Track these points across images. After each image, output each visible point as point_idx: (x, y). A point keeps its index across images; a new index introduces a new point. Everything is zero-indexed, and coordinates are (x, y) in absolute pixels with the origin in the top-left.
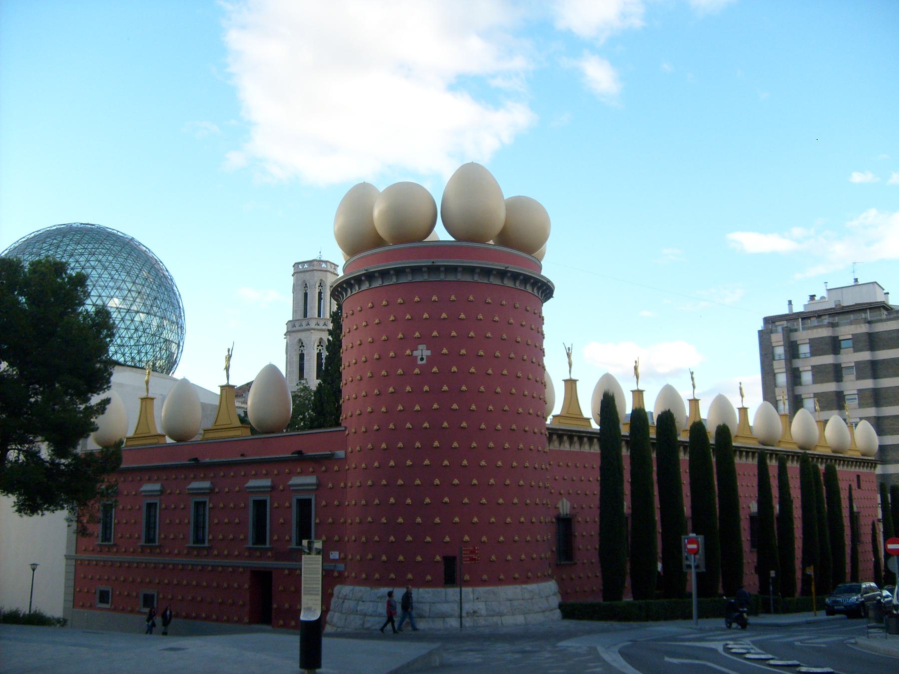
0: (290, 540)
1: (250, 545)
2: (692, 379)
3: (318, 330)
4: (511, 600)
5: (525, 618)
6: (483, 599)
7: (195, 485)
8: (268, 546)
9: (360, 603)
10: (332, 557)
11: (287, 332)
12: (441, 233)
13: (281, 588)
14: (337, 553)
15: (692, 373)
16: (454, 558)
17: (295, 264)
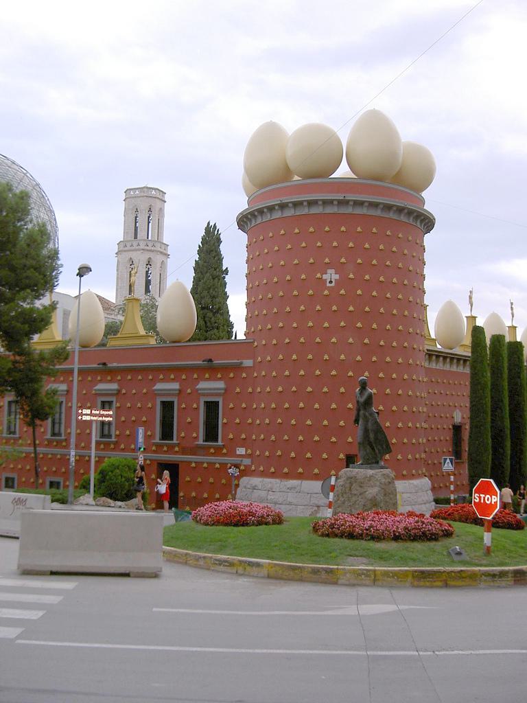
0: (196, 438)
1: (157, 440)
2: (512, 308)
3: (148, 250)
7: (101, 386)
8: (175, 441)
10: (238, 453)
11: (119, 251)
12: (343, 171)
14: (244, 449)
15: (512, 304)
16: (356, 455)
17: (128, 190)
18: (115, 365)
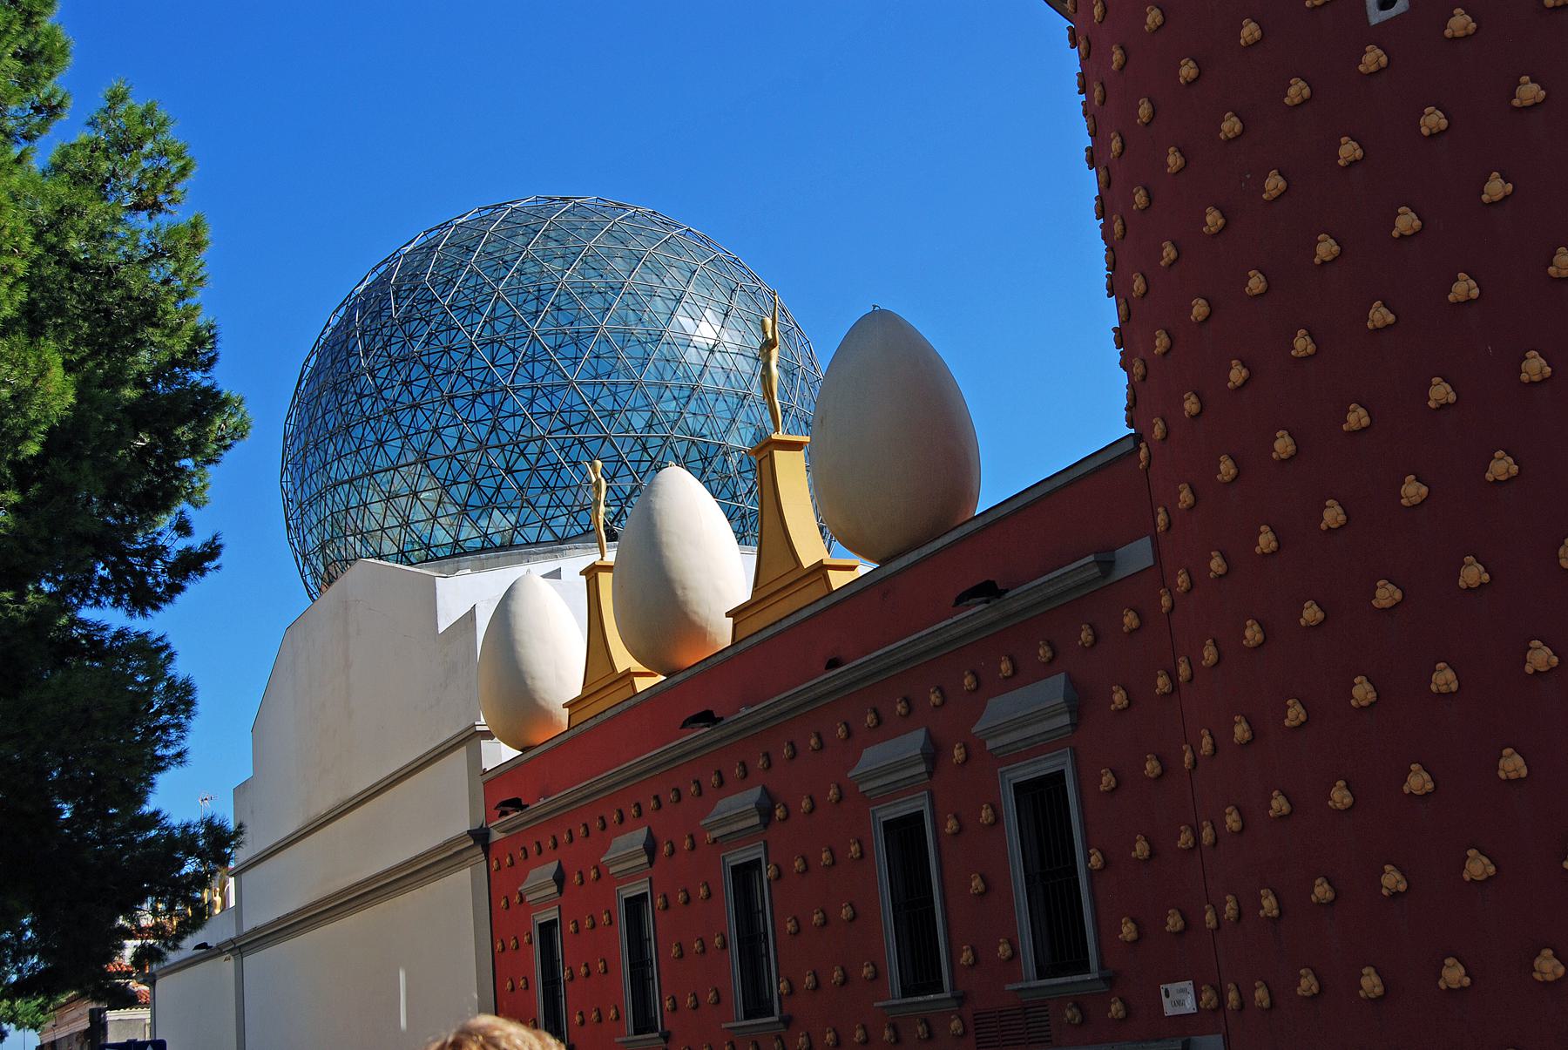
10: (1169, 1009)
14: (1188, 985)
18: (744, 711)
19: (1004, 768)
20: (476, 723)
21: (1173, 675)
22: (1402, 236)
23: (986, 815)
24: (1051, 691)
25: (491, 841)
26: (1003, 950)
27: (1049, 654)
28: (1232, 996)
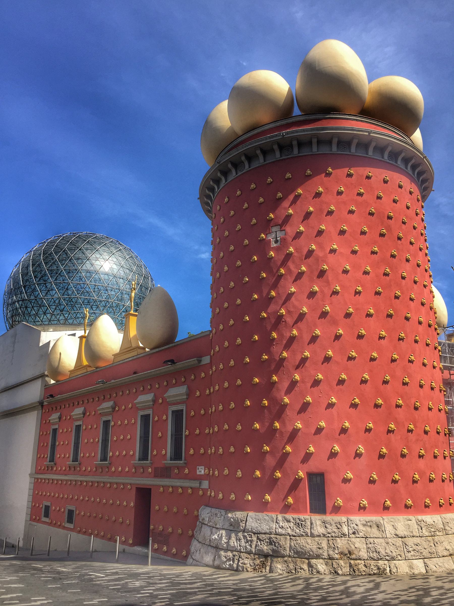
4: (402, 538)
5: (426, 565)
6: (361, 534)
9: (214, 530)
13: (157, 508)
14: (203, 467)
16: (321, 475)
19: (170, 406)
20: (45, 372)
21: (210, 391)
22: (271, 297)
23: (164, 417)
24: (183, 389)
25: (44, 404)
26: (164, 452)
27: (184, 380)
28: (211, 472)
